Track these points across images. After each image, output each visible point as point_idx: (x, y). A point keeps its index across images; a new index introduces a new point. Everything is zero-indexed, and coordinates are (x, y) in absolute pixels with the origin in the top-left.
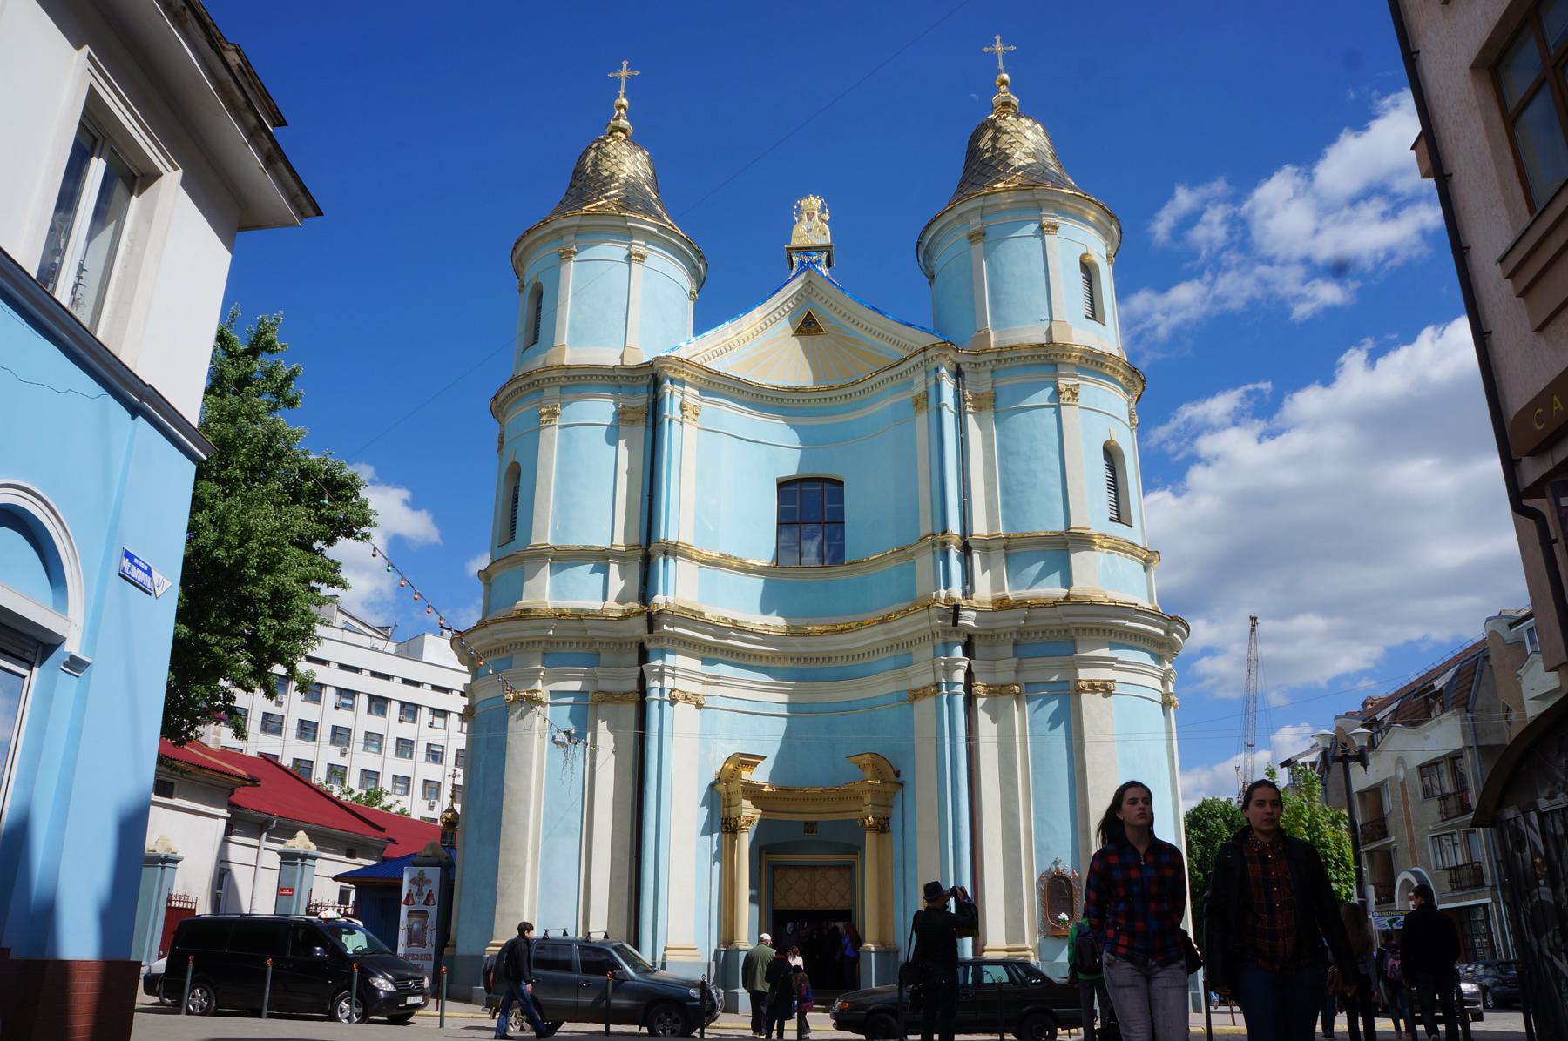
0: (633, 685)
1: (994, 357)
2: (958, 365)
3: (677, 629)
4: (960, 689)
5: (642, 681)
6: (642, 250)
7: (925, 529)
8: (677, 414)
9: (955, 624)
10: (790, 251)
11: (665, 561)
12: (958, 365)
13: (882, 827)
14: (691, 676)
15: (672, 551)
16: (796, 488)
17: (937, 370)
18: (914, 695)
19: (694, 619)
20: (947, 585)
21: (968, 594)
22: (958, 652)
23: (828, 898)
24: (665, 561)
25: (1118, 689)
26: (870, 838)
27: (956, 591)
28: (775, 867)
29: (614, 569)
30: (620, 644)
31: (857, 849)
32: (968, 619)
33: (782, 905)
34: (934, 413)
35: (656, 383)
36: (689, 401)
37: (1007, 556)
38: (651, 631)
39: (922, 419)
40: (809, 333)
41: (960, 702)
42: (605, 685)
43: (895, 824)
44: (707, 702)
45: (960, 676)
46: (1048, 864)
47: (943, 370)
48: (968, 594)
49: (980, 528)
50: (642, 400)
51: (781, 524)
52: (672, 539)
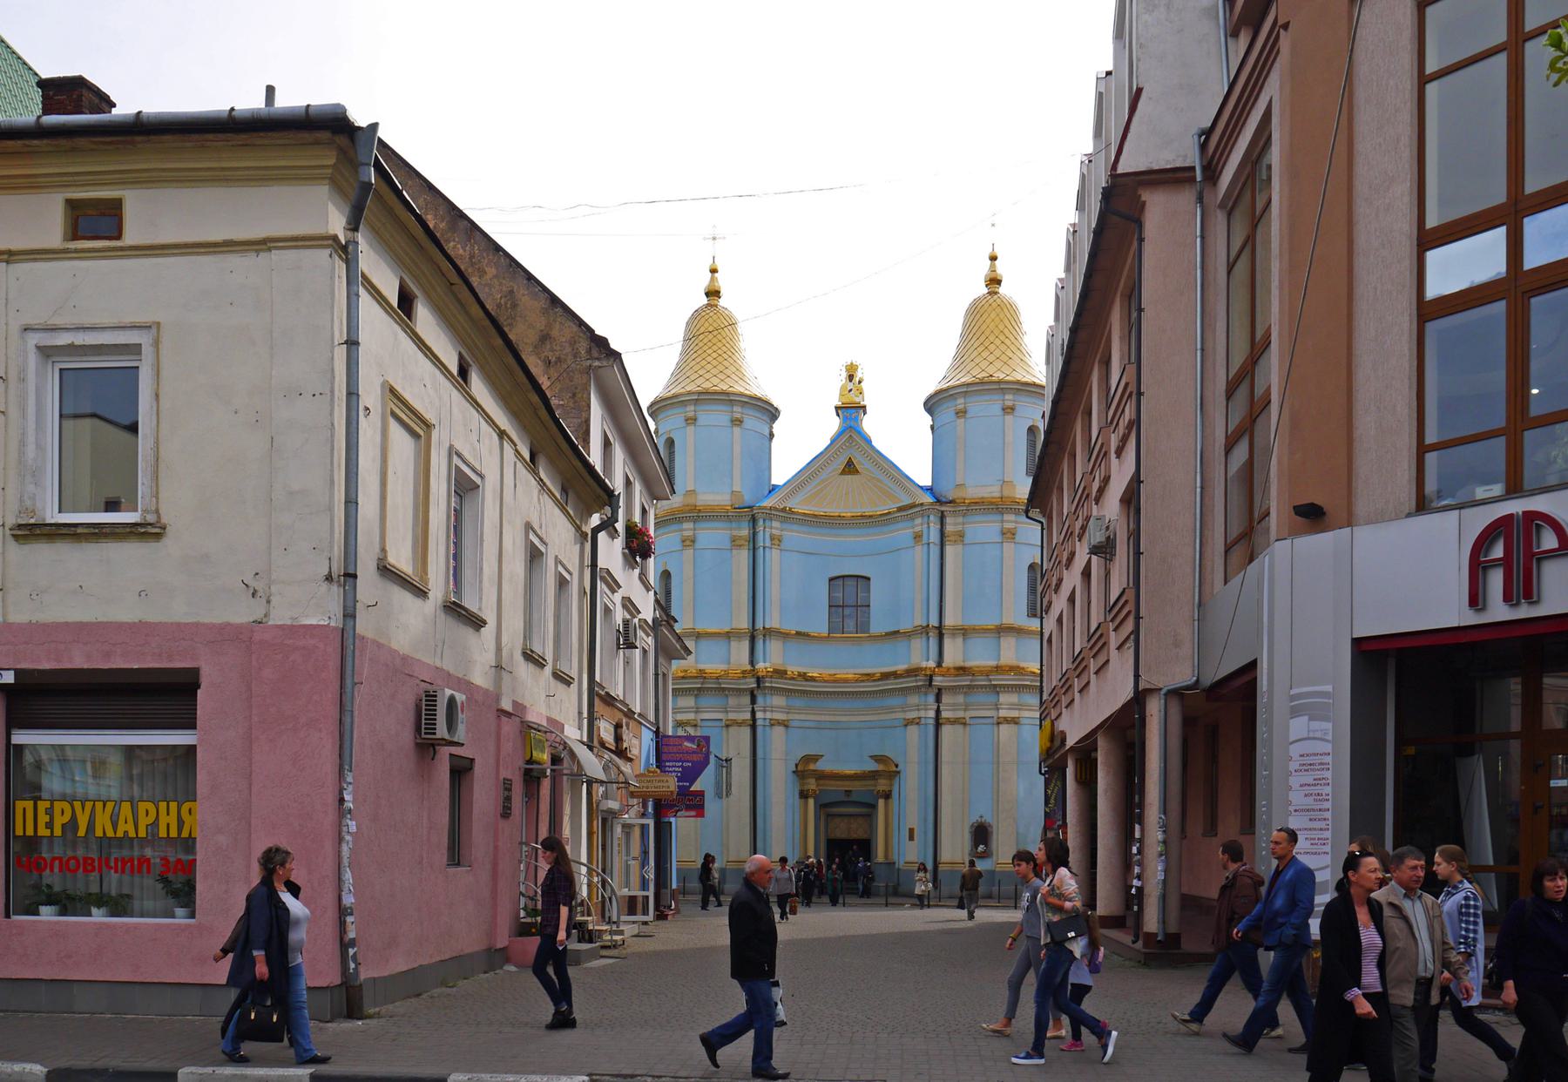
0: (748, 716)
4: (932, 721)
5: (753, 713)
7: (919, 621)
8: (768, 544)
10: (837, 408)
13: (887, 796)
14: (779, 709)
15: (769, 633)
16: (840, 582)
18: (908, 723)
21: (939, 664)
22: (931, 699)
23: (857, 831)
25: (1023, 721)
26: (881, 802)
27: (932, 664)
28: (828, 815)
30: (739, 692)
31: (874, 807)
32: (938, 681)
33: (832, 836)
35: (754, 520)
39: (918, 548)
40: (850, 473)
41: (931, 729)
42: (732, 716)
44: (792, 724)
45: (932, 714)
46: (974, 819)
48: (939, 664)
49: (949, 621)
50: (745, 532)
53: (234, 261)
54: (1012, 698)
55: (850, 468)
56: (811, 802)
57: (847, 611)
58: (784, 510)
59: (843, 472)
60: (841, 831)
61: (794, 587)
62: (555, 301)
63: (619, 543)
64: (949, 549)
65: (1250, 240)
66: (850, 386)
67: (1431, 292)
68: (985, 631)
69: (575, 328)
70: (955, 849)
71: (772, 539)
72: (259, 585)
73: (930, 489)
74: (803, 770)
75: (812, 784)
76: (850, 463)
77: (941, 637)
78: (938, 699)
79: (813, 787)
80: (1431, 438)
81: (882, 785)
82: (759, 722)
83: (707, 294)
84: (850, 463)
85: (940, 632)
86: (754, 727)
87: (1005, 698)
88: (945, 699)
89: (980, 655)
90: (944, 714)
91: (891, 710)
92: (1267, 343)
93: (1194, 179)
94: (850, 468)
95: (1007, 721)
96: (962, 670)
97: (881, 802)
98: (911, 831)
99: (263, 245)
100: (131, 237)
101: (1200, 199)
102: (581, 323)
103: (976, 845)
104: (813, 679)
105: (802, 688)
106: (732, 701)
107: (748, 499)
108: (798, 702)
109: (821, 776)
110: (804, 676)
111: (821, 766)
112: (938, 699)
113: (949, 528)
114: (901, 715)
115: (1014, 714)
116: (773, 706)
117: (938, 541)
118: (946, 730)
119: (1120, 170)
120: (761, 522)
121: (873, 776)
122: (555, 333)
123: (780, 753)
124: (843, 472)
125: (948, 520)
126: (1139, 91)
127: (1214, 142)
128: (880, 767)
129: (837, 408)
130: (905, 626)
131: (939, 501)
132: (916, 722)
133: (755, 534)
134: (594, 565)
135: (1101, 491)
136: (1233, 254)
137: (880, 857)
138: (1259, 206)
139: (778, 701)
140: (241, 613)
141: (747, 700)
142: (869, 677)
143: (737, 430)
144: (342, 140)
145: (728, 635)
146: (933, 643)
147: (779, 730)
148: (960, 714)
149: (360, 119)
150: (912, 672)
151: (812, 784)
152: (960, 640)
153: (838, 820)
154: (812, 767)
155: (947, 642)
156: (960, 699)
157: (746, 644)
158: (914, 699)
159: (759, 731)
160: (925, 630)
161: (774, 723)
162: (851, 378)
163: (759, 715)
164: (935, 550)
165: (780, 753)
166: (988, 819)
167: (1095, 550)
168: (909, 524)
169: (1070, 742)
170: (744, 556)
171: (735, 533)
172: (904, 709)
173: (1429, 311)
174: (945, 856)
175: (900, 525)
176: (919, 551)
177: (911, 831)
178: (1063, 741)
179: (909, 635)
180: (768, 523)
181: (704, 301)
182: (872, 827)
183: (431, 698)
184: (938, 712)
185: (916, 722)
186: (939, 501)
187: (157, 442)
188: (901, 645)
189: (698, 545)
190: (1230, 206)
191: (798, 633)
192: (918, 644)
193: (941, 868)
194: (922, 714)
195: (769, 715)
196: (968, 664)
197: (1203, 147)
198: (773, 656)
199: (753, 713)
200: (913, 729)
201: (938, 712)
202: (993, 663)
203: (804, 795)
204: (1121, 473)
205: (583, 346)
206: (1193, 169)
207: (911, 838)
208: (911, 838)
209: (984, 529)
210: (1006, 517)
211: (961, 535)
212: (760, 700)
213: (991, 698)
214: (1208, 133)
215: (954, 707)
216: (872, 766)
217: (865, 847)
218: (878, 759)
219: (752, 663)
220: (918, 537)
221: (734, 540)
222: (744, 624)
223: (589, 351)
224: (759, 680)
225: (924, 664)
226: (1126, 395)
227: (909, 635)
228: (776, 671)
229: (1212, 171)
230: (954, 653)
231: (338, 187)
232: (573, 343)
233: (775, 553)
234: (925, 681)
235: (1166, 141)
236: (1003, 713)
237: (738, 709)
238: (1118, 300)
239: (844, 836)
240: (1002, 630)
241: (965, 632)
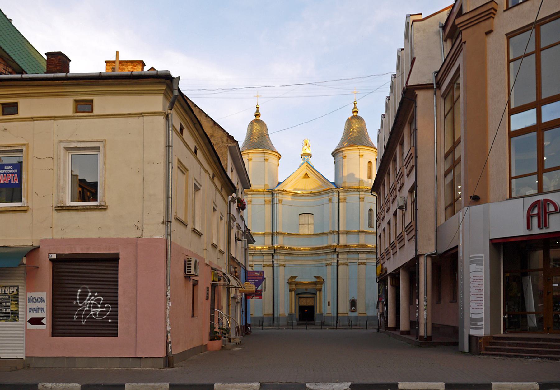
0: (271, 263)
4: (336, 264)
5: (273, 262)
13: (320, 290)
15: (278, 233)
19: (282, 248)
21: (338, 244)
22: (335, 256)
23: (309, 303)
26: (318, 292)
27: (335, 244)
29: (266, 238)
31: (315, 294)
32: (338, 250)
33: (301, 305)
35: (273, 194)
36: (280, 198)
39: (331, 204)
40: (306, 178)
41: (336, 267)
42: (265, 263)
43: (323, 290)
44: (286, 265)
45: (336, 261)
46: (351, 298)
48: (338, 244)
49: (341, 229)
53: (131, 120)
54: (364, 256)
55: (306, 176)
56: (293, 292)
58: (283, 191)
59: (304, 178)
60: (304, 303)
62: (215, 123)
63: (236, 204)
65: (452, 108)
66: (305, 147)
67: (513, 128)
68: (355, 232)
69: (222, 133)
70: (344, 308)
71: (279, 201)
72: (139, 225)
73: (333, 183)
74: (292, 282)
75: (294, 287)
76: (306, 174)
77: (339, 234)
78: (338, 257)
79: (294, 287)
80: (513, 175)
81: (318, 286)
82: (275, 265)
83: (256, 115)
84: (306, 174)
85: (338, 233)
86: (273, 267)
87: (361, 256)
88: (340, 256)
89: (352, 241)
90: (340, 262)
91: (321, 260)
92: (459, 141)
93: (433, 88)
94: (306, 176)
95: (362, 264)
96: (346, 246)
97: (318, 292)
98: (329, 303)
99: (141, 114)
100: (96, 112)
101: (435, 94)
102: (224, 131)
103: (351, 307)
104: (294, 250)
105: (291, 252)
106: (266, 257)
107: (270, 187)
108: (288, 258)
109: (297, 284)
110: (290, 248)
111: (297, 280)
112: (338, 257)
113: (341, 197)
114: (324, 262)
115: (365, 261)
116: (279, 258)
118: (340, 267)
119: (409, 84)
121: (315, 283)
122: (215, 134)
123: (283, 275)
124: (304, 178)
126: (415, 58)
127: (440, 76)
128: (318, 280)
129: (301, 155)
130: (326, 231)
131: (337, 187)
132: (330, 264)
134: (230, 213)
135: (401, 188)
136: (446, 113)
137: (318, 312)
138: (455, 97)
139: (281, 257)
140: (133, 234)
141: (271, 257)
142: (313, 249)
144: (168, 81)
146: (336, 236)
147: (282, 268)
148: (345, 261)
149: (174, 75)
150: (329, 247)
151: (294, 287)
152: (345, 236)
153: (302, 299)
154: (294, 280)
155: (340, 236)
156: (345, 256)
157: (270, 237)
158: (329, 256)
159: (275, 268)
161: (280, 265)
162: (306, 145)
163: (275, 262)
164: (336, 205)
165: (283, 275)
166: (355, 298)
167: (400, 208)
168: (327, 195)
169: (389, 272)
170: (269, 207)
172: (326, 260)
173: (513, 134)
174: (341, 311)
175: (324, 196)
177: (329, 303)
178: (386, 271)
179: (327, 234)
181: (254, 118)
182: (315, 301)
183: (190, 261)
184: (338, 261)
185: (330, 264)
186: (337, 187)
187: (105, 179)
188: (325, 237)
189: (252, 203)
190: (444, 96)
191: (288, 234)
192: (331, 237)
193: (339, 315)
194: (332, 261)
195: (278, 263)
196: (348, 244)
197: (436, 77)
198: (280, 241)
199: (273, 262)
200: (329, 267)
201: (338, 261)
202: (357, 244)
203: (291, 290)
204: (409, 183)
205: (225, 139)
206: (433, 84)
207: (329, 305)
208: (329, 305)
209: (354, 197)
210: (361, 193)
212: (275, 257)
213: (356, 256)
214: (438, 72)
215: (343, 259)
216: (314, 280)
217: (311, 309)
218: (317, 277)
219: (272, 244)
220: (330, 200)
222: (269, 230)
223: (227, 140)
224: (275, 251)
225: (333, 244)
226: (411, 157)
227: (327, 234)
228: (281, 247)
229: (439, 85)
231: (166, 96)
232: (221, 138)
233: (280, 205)
234: (334, 250)
235: (423, 74)
236: (360, 261)
237: (268, 260)
238: (407, 124)
239: (305, 305)
240: (360, 232)
241: (347, 233)
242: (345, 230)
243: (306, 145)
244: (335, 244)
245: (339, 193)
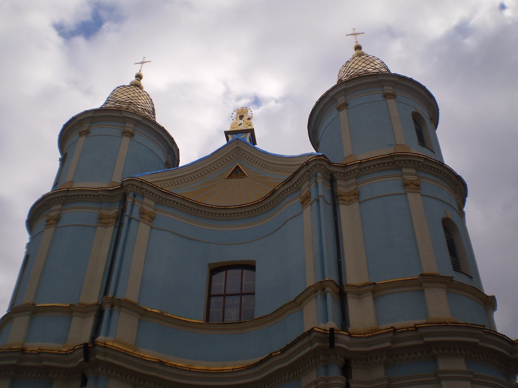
1: (356, 167)
2: (332, 175)
3: (109, 359)
6: (131, 130)
7: (311, 281)
8: (136, 214)
9: (332, 345)
10: (227, 133)
11: (111, 312)
12: (332, 175)
15: (118, 304)
17: (316, 176)
20: (326, 320)
22: (335, 371)
24: (111, 312)
29: (76, 320)
32: (342, 341)
34: (315, 203)
37: (374, 299)
38: (87, 359)
39: (307, 211)
47: (319, 175)
50: (114, 210)
51: (210, 296)
52: (118, 296)
57: (229, 300)
59: (230, 176)
61: (162, 263)
64: (344, 210)
66: (241, 121)
71: (142, 213)
77: (342, 296)
94: (237, 172)
96: (374, 334)
117: (329, 199)
120: (131, 195)
125: (339, 182)
133: (123, 210)
143: (126, 140)
145: (70, 311)
152: (368, 300)
155: (352, 303)
160: (320, 288)
162: (241, 117)
164: (326, 210)
170: (109, 232)
171: (102, 211)
176: (309, 212)
180: (138, 198)
189: (59, 225)
198: (121, 333)
211: (356, 194)
221: (100, 218)
230: (362, 315)
240: (428, 279)
241: (374, 290)
242: (365, 279)
243: (241, 117)
244: (331, 324)
245: (332, 181)
